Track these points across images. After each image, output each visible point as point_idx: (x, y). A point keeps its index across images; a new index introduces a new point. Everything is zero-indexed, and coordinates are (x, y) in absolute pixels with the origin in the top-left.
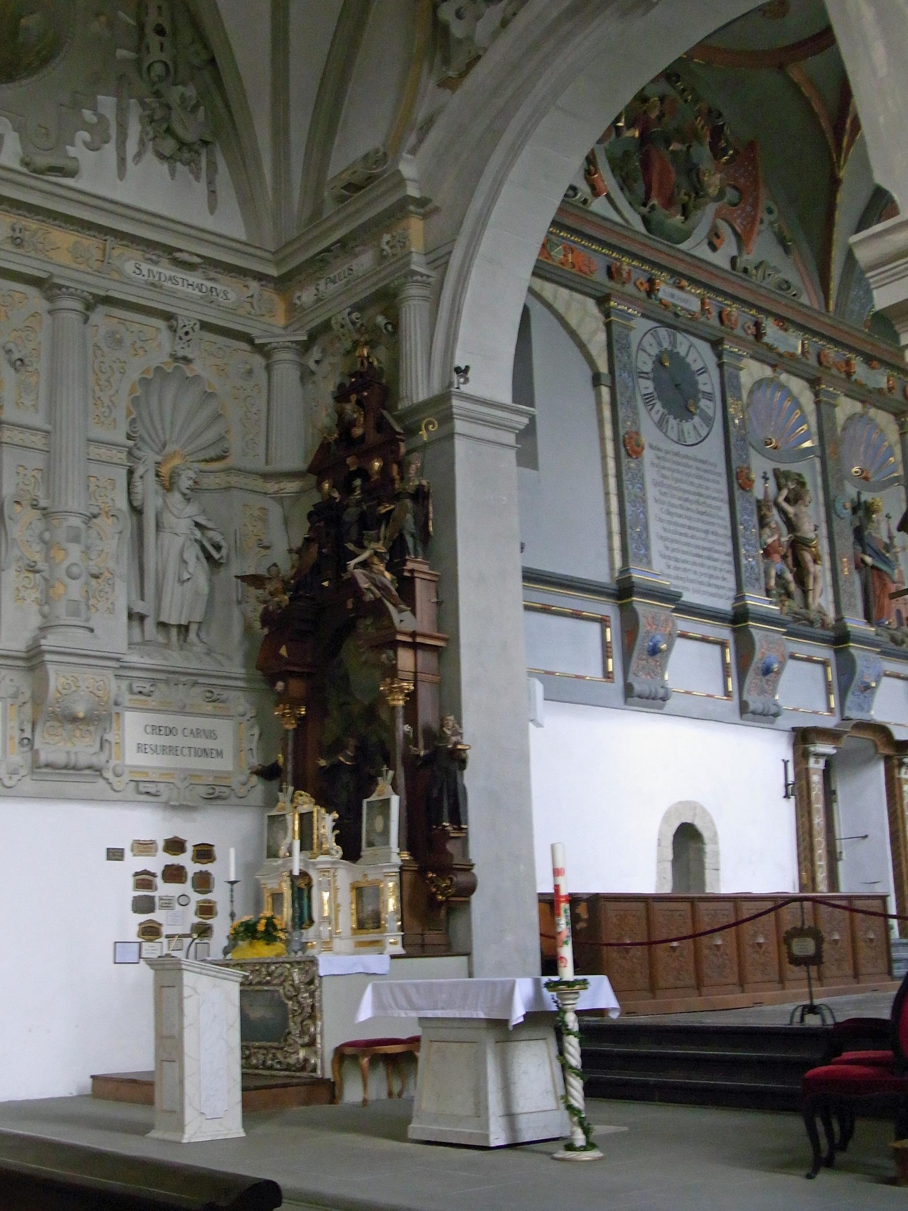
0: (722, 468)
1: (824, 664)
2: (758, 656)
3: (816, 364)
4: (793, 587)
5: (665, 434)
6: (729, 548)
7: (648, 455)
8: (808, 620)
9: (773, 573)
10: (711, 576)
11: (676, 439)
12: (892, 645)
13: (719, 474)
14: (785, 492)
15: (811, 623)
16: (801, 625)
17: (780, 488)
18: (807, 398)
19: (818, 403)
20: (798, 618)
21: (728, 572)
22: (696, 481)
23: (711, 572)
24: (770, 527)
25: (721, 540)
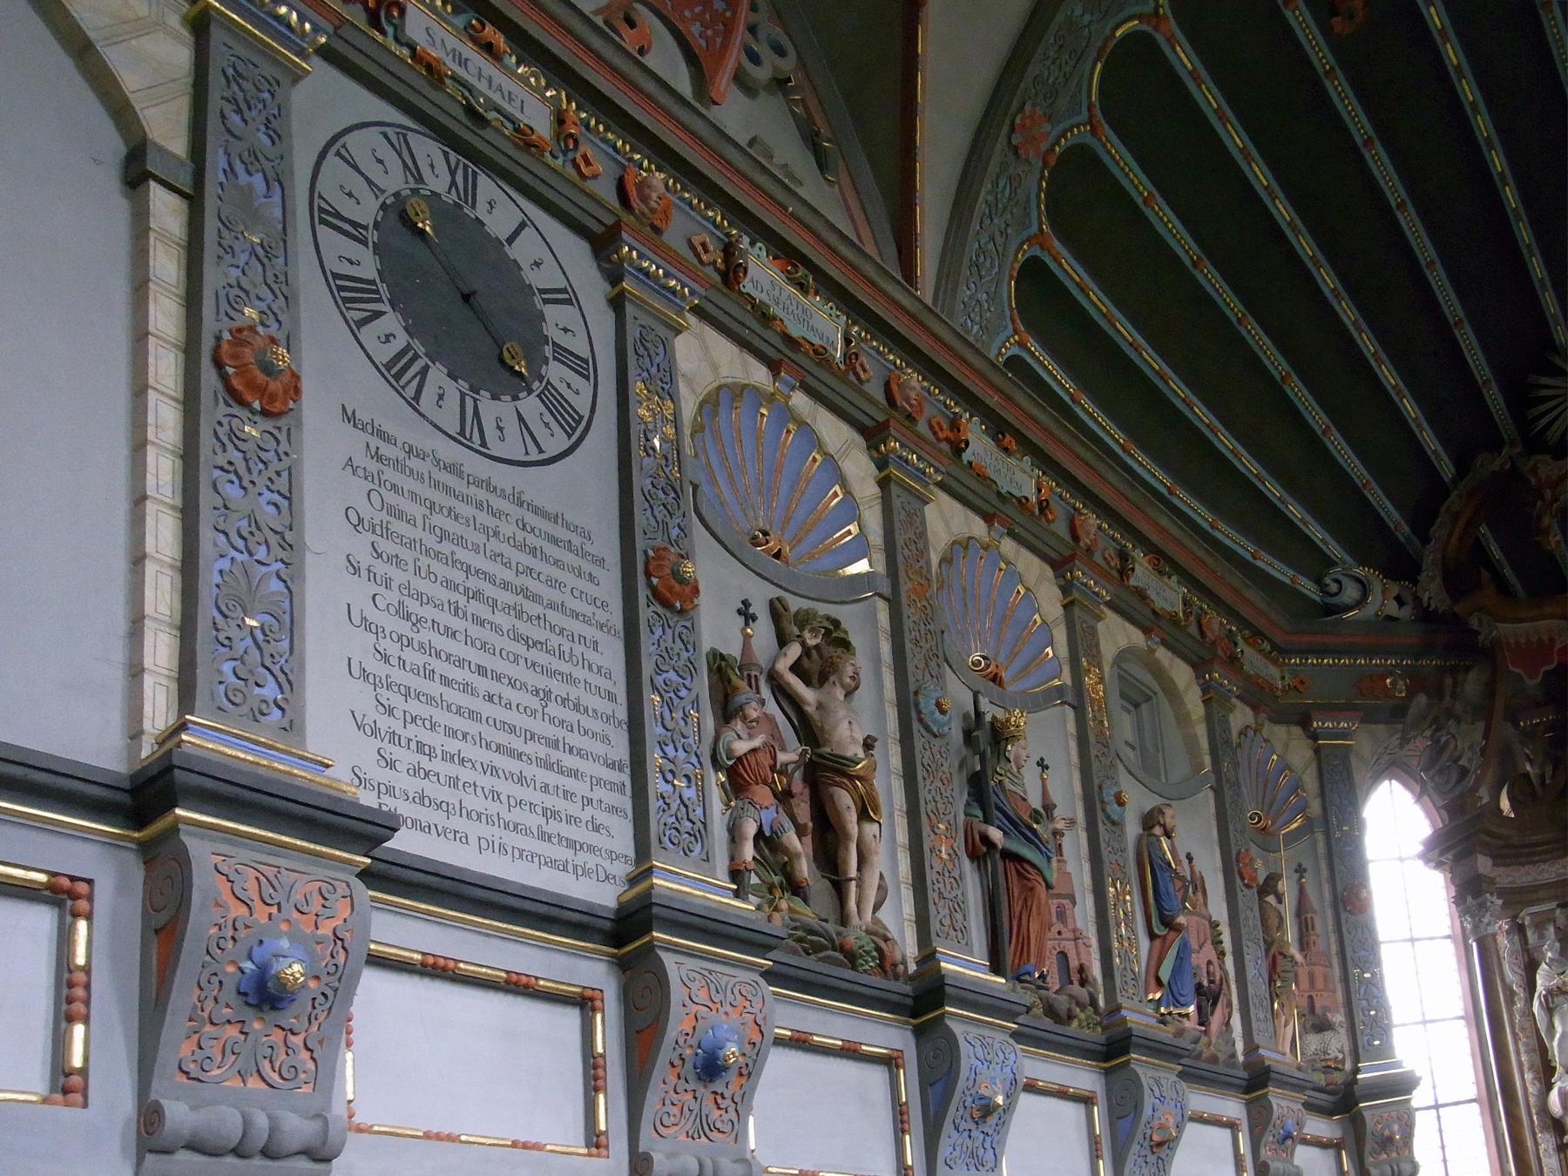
0: (607, 544)
1: (890, 1062)
3: (880, 397)
4: (805, 868)
5: (414, 403)
6: (620, 749)
7: (316, 411)
8: (842, 949)
9: (751, 829)
11: (454, 429)
12: (1047, 1023)
13: (601, 562)
14: (794, 651)
15: (852, 958)
16: (824, 963)
17: (783, 641)
18: (859, 467)
19: (884, 483)
20: (810, 940)
21: (612, 809)
22: (516, 556)
24: (744, 718)
25: (596, 726)
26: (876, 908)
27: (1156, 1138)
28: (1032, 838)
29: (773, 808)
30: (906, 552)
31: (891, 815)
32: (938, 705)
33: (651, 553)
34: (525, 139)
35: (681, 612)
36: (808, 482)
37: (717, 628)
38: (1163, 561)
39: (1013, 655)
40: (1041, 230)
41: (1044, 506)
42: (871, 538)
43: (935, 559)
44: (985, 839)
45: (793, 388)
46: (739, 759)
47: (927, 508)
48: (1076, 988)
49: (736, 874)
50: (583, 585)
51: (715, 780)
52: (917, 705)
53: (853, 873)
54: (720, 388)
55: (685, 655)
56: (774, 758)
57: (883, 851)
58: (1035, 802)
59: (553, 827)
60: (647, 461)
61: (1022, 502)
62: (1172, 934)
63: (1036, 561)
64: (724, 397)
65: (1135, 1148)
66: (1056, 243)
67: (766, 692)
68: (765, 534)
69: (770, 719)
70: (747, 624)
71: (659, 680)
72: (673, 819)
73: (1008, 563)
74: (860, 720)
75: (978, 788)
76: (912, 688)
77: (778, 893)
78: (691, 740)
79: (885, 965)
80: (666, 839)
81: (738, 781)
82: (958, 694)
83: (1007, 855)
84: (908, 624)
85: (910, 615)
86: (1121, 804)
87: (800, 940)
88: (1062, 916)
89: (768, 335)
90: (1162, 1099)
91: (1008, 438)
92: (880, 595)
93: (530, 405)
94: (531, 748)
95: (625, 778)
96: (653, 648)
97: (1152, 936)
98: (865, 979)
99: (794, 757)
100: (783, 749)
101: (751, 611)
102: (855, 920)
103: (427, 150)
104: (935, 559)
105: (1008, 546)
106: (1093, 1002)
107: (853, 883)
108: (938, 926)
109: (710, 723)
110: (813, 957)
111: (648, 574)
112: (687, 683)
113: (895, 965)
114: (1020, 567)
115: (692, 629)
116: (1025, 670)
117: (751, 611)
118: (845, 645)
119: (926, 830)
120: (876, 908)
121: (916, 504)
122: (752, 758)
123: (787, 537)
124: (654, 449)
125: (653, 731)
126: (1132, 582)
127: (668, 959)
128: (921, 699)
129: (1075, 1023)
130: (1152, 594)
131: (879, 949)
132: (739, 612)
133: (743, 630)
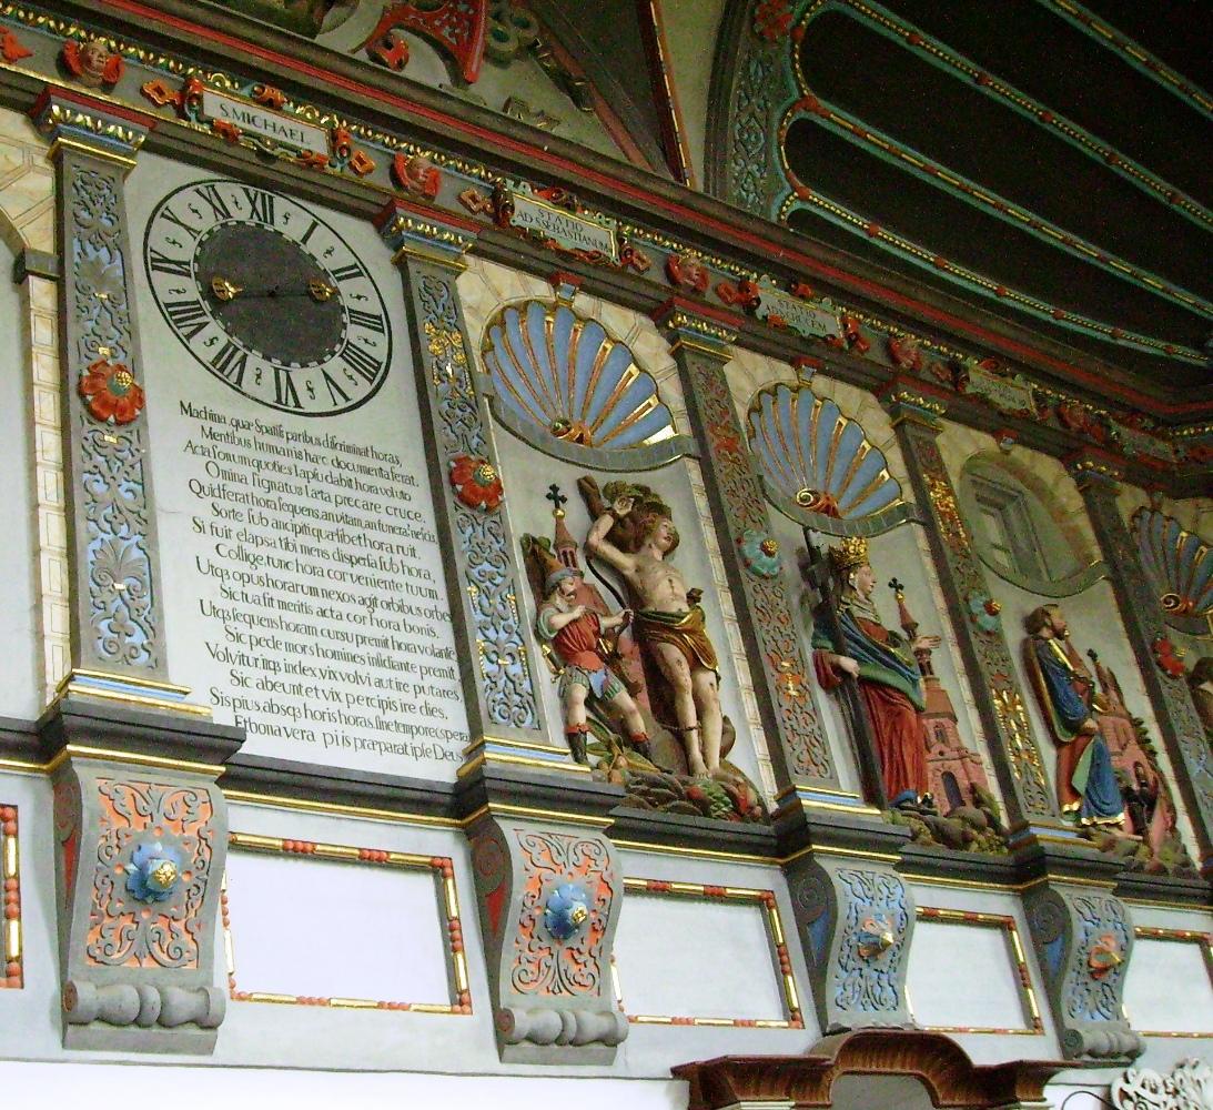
1: (763, 902)
2: (520, 891)
4: (640, 724)
6: (446, 639)
8: (689, 797)
9: (580, 693)
10: (385, 705)
12: (940, 849)
13: (411, 480)
14: (606, 523)
15: (703, 806)
16: (670, 810)
17: (595, 515)
18: (651, 347)
19: (677, 354)
20: (651, 793)
21: (444, 693)
23: (384, 694)
25: (421, 622)
26: (724, 752)
27: (1095, 963)
28: (892, 664)
29: (601, 671)
30: (709, 412)
31: (730, 659)
32: (764, 548)
33: (453, 464)
34: (308, 162)
35: (488, 510)
36: (601, 369)
37: (525, 515)
38: (1000, 362)
39: (845, 484)
40: (803, 96)
41: (853, 339)
42: (672, 406)
43: (741, 411)
44: (838, 669)
45: (574, 294)
46: (562, 630)
48: (970, 810)
49: (573, 737)
50: (397, 502)
51: (540, 654)
53: (692, 721)
54: (504, 309)
55: (496, 546)
56: (598, 624)
57: (727, 694)
58: (892, 623)
59: (390, 716)
60: (442, 387)
61: (829, 341)
62: (1082, 741)
63: (856, 391)
64: (511, 317)
65: (1070, 976)
66: (823, 104)
67: (582, 564)
68: (565, 423)
69: (591, 589)
70: (557, 506)
71: (474, 573)
72: (501, 695)
73: (823, 399)
74: (686, 574)
75: (826, 620)
76: (733, 536)
77: (616, 750)
78: (511, 622)
79: (740, 808)
80: (496, 715)
81: (564, 649)
82: (786, 530)
83: (865, 681)
84: (720, 478)
85: (722, 468)
86: (993, 613)
87: (644, 793)
88: (941, 735)
89: (541, 254)
90: (1096, 921)
91: (802, 286)
92: (689, 456)
93: (335, 365)
94: (363, 650)
95: (453, 663)
96: (464, 546)
97: (1058, 744)
98: (721, 824)
99: (617, 620)
100: (608, 614)
101: (560, 494)
102: (701, 767)
103: (231, 192)
104: (741, 411)
105: (821, 384)
106: (993, 822)
107: (694, 734)
108: (795, 762)
109: (528, 601)
110: (661, 808)
111: (453, 484)
112: (501, 571)
113: (752, 808)
114: (838, 400)
115: (502, 522)
116: (862, 496)
117: (560, 494)
118: (661, 510)
119: (769, 670)
120: (724, 752)
121: (713, 366)
122: (574, 629)
123: (589, 422)
124: (447, 375)
125: (474, 618)
126: (969, 390)
127: (507, 827)
128: (746, 548)
129: (974, 846)
130: (994, 397)
131: (729, 793)
132: (549, 497)
133: (554, 513)
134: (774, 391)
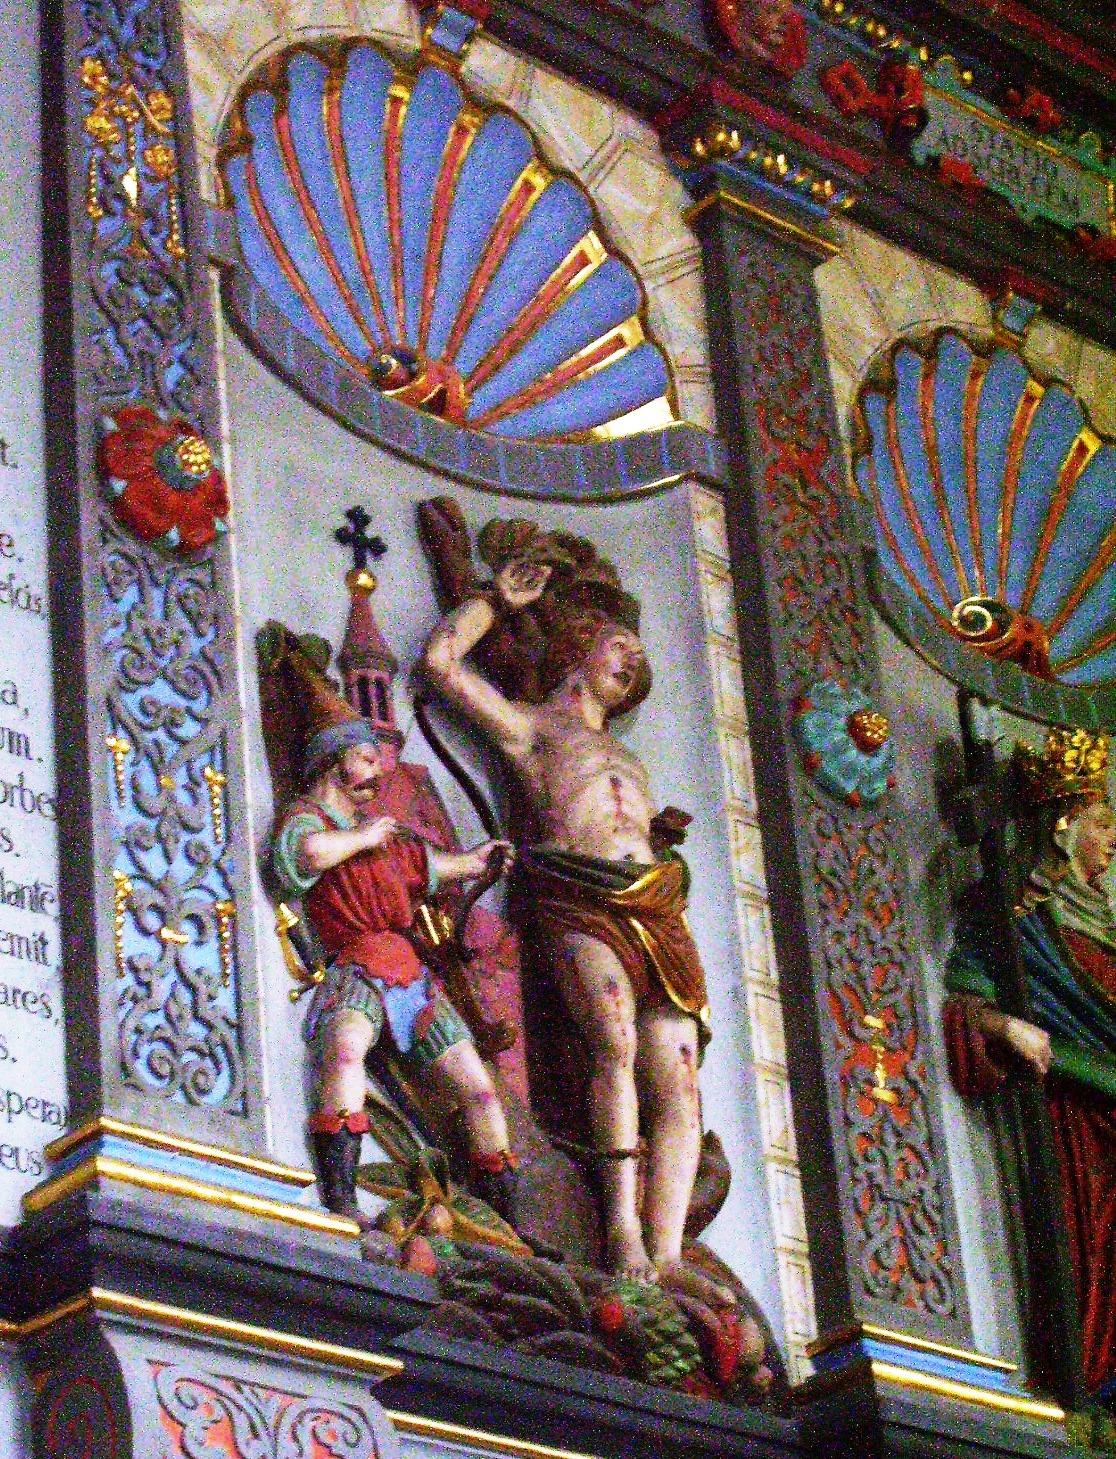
4: (495, 1129)
8: (598, 1325)
9: (357, 1035)
14: (475, 619)
17: (449, 593)
18: (643, 199)
19: (704, 224)
20: (503, 1303)
24: (345, 778)
26: (700, 1218)
29: (417, 987)
30: (763, 377)
31: (738, 995)
32: (854, 729)
33: (110, 425)
35: (185, 552)
36: (514, 235)
37: (277, 572)
39: (1069, 606)
42: (675, 350)
43: (844, 385)
45: (469, 38)
46: (331, 875)
47: (822, 276)
49: (328, 1143)
51: (267, 925)
52: (797, 731)
53: (627, 1135)
54: (287, 54)
55: (194, 645)
56: (422, 868)
57: (723, 1080)
60: (106, 226)
64: (304, 75)
67: (403, 714)
68: (406, 358)
69: (417, 778)
70: (360, 564)
71: (130, 702)
72: (159, 1019)
73: (1048, 382)
74: (658, 766)
76: (785, 690)
77: (431, 1188)
78: (205, 837)
80: (140, 1067)
81: (334, 922)
83: (1061, 1085)
84: (770, 541)
85: (775, 521)
87: (484, 1304)
91: (1035, 95)
92: (702, 480)
95: (47, 924)
96: (113, 634)
98: (660, 1399)
99: (471, 864)
100: (451, 845)
101: (370, 532)
102: (636, 1255)
104: (844, 385)
107: (628, 1170)
108: (867, 1266)
109: (257, 791)
110: (522, 1345)
111: (104, 473)
112: (198, 706)
113: (748, 1368)
115: (215, 585)
117: (370, 532)
118: (617, 607)
119: (830, 1033)
120: (700, 1218)
121: (787, 267)
122: (362, 872)
123: (465, 364)
124: (122, 198)
125: (114, 816)
127: (132, 1355)
128: (811, 723)
131: (695, 1325)
132: (342, 536)
133: (351, 577)
134: (930, 346)
